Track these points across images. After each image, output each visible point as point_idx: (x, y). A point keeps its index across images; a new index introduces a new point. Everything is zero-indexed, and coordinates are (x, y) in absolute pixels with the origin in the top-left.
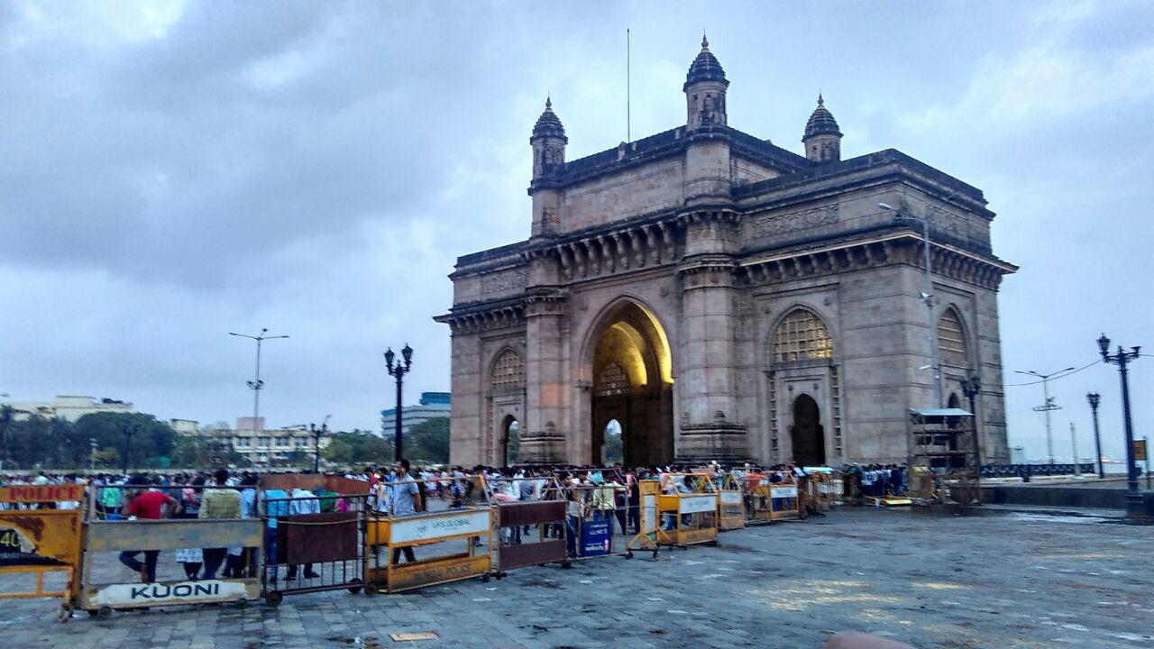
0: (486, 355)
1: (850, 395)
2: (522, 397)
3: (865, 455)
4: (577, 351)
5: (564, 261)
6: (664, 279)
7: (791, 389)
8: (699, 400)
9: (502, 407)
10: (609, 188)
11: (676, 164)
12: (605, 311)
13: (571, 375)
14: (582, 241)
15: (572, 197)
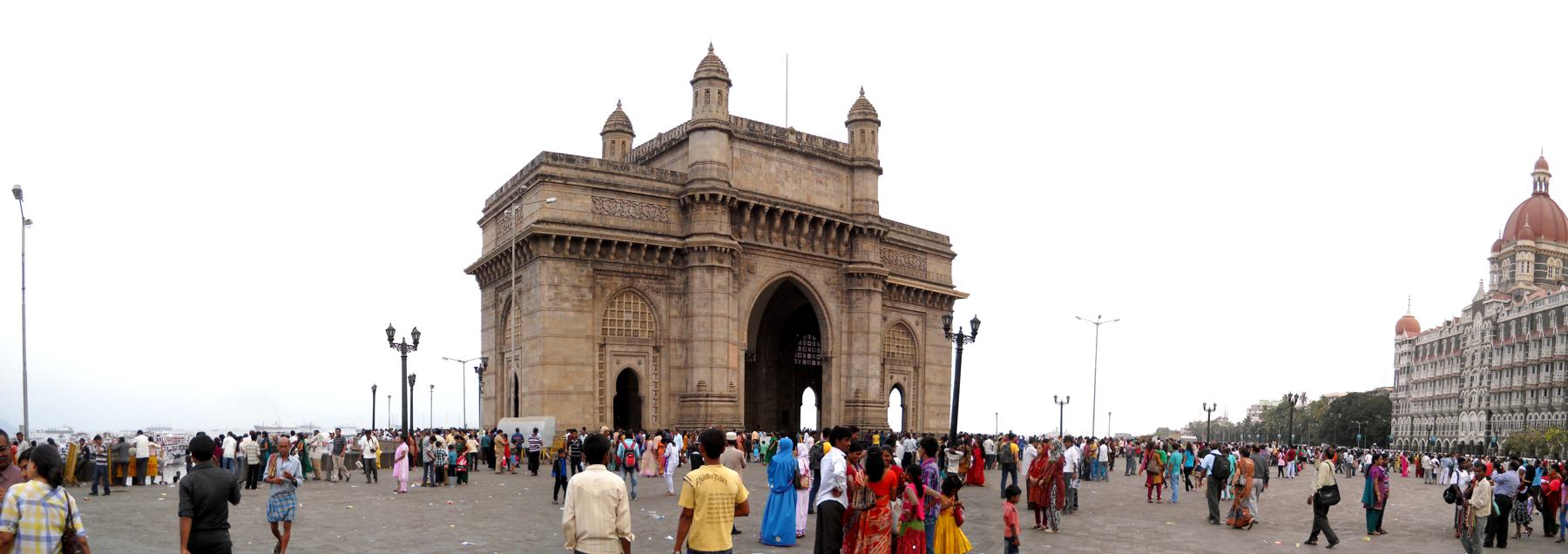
0: (598, 290)
1: (927, 387)
2: (651, 351)
3: (931, 427)
4: (742, 314)
5: (748, 217)
6: (829, 270)
7: (892, 378)
8: (874, 380)
9: (620, 358)
10: (781, 161)
11: (844, 174)
12: (770, 282)
13: (739, 336)
14: (777, 207)
15: (742, 151)
